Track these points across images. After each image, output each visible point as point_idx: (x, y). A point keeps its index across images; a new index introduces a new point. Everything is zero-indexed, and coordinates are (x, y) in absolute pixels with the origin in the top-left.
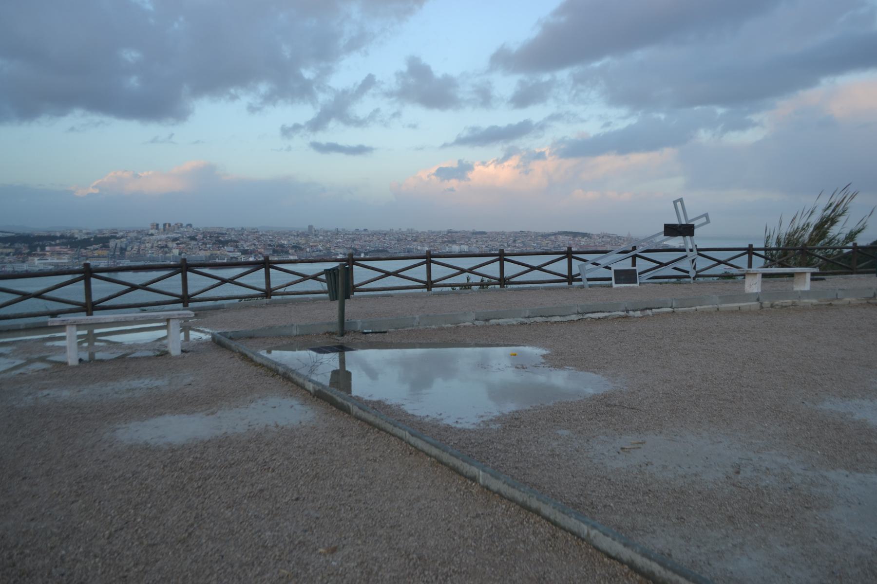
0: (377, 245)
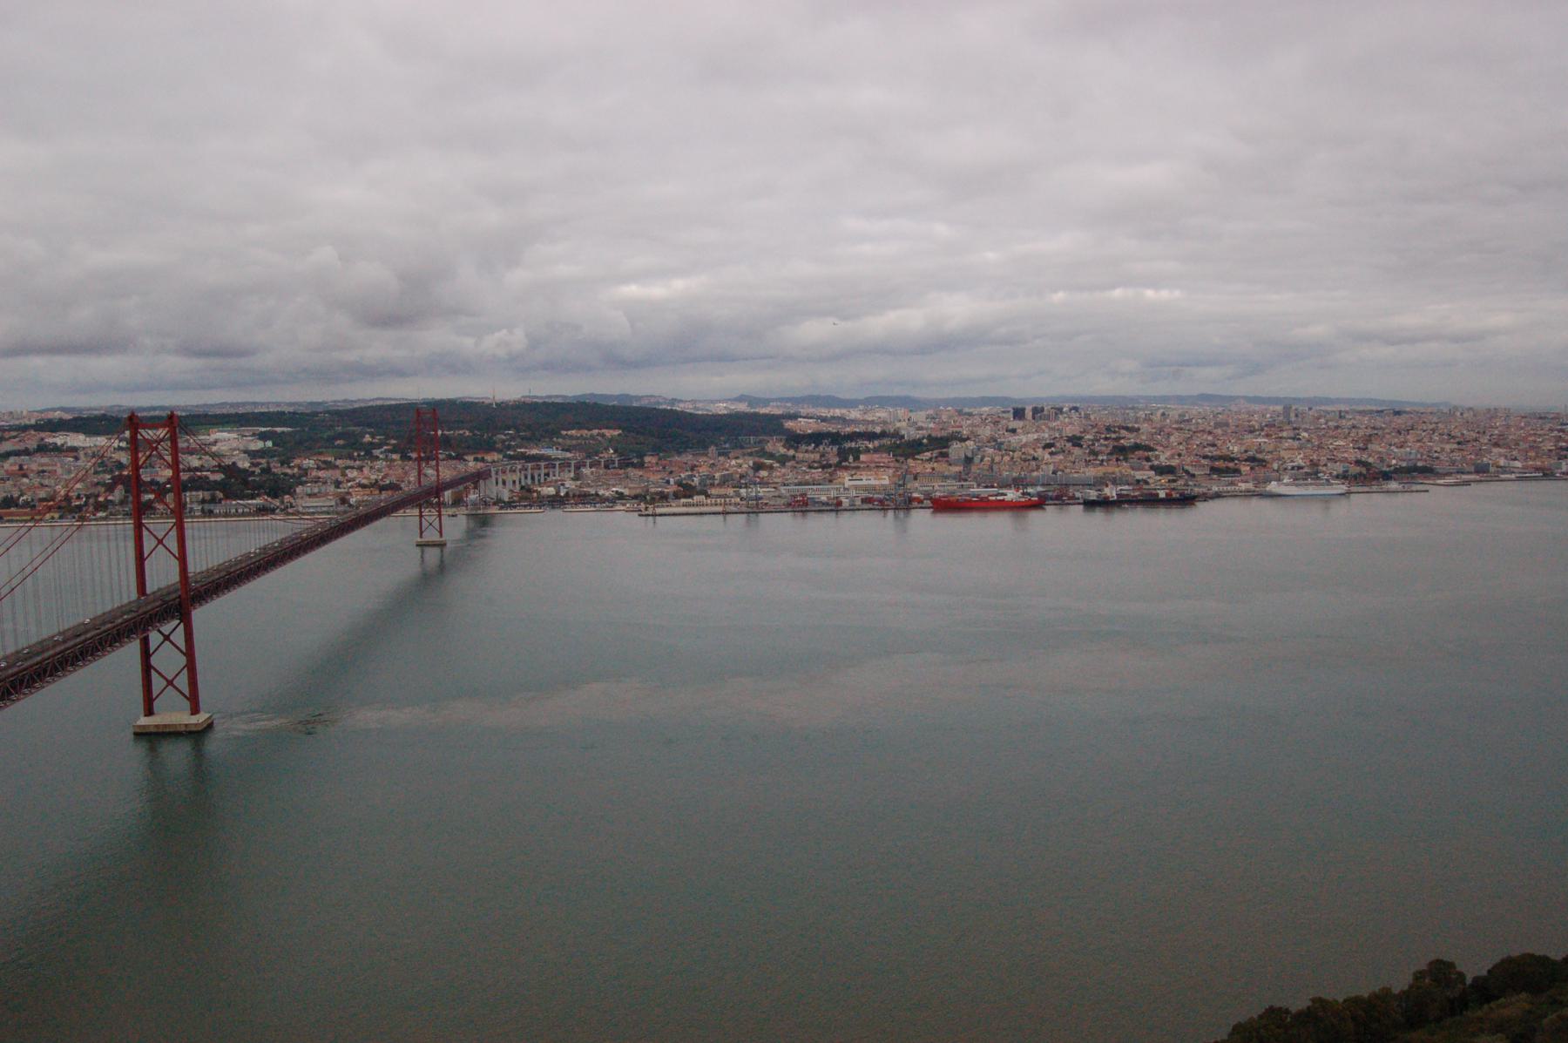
0: (1412, 457)
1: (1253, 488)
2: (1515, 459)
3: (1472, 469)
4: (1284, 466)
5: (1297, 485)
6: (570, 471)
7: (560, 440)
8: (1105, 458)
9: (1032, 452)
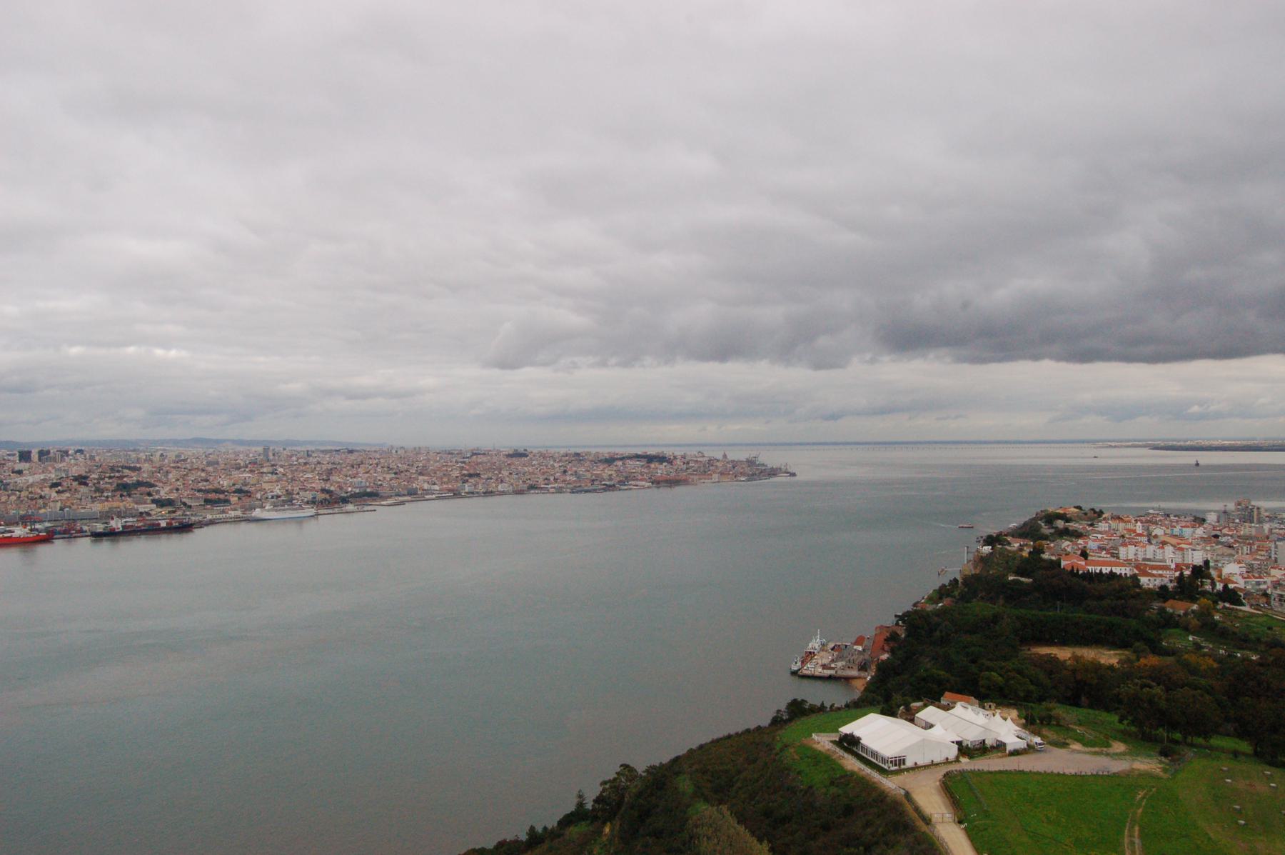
0: (363, 484)
1: (241, 515)
2: (434, 484)
3: (406, 492)
4: (266, 496)
5: (276, 511)
8: (110, 494)
9: (39, 491)
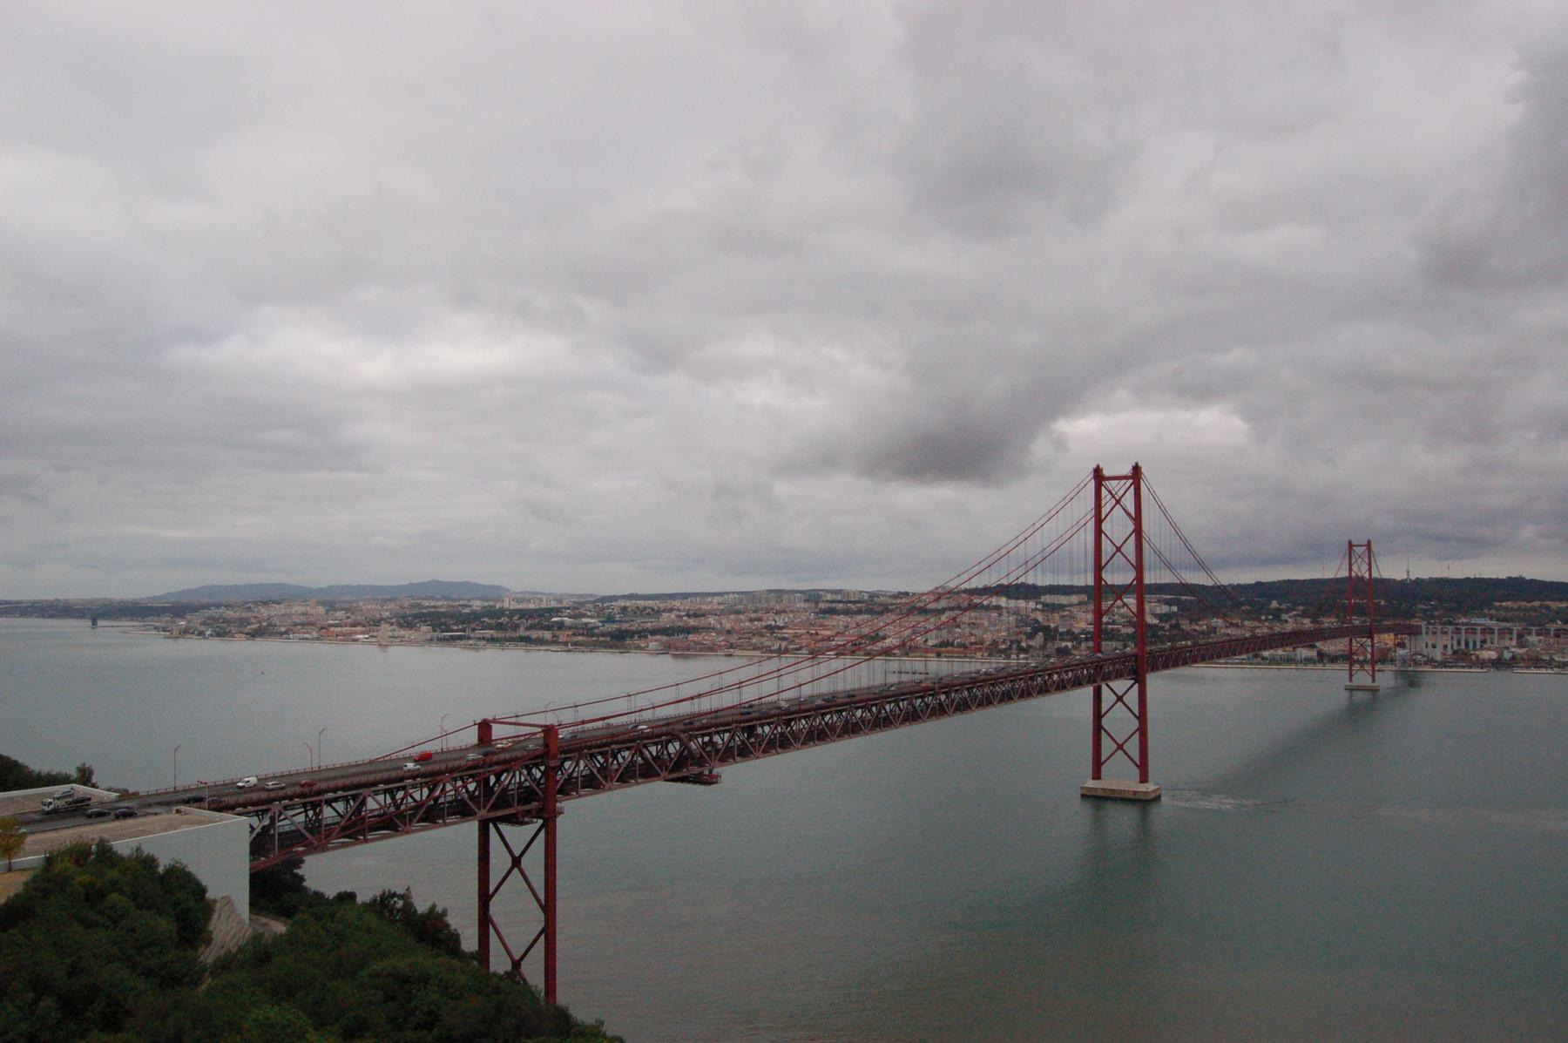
6: (1511, 639)
7: (1493, 612)
